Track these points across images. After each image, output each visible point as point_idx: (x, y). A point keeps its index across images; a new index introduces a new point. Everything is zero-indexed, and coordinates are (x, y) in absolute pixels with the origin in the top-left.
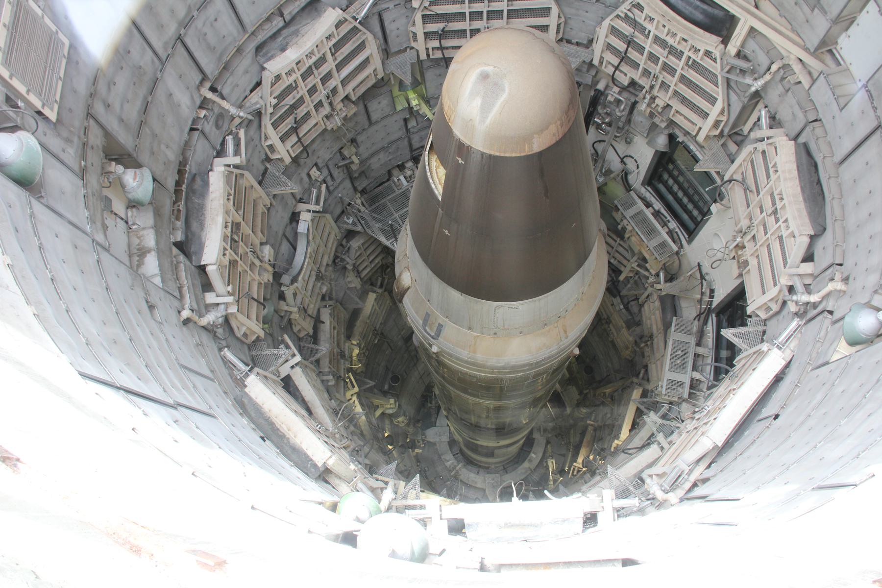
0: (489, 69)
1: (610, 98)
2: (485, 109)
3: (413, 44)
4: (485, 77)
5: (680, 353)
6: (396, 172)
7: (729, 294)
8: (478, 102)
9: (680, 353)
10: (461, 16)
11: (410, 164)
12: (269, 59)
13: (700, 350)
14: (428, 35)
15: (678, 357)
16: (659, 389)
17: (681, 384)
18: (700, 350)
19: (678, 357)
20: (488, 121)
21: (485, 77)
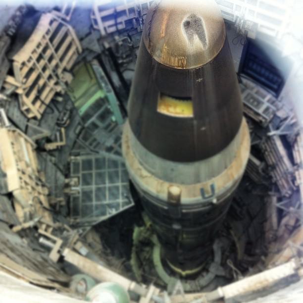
0: (185, 19)
1: (120, 43)
2: (202, 37)
3: (30, 115)
4: (187, 24)
5: (251, 101)
6: (67, 191)
7: (241, 58)
8: (196, 38)
9: (251, 101)
10: (39, 77)
11: (67, 181)
12: (6, 186)
13: (255, 90)
14: (34, 103)
15: (253, 102)
16: (263, 120)
17: (267, 109)
18: (255, 90)
19: (253, 102)
20: (207, 41)
21: (187, 24)
